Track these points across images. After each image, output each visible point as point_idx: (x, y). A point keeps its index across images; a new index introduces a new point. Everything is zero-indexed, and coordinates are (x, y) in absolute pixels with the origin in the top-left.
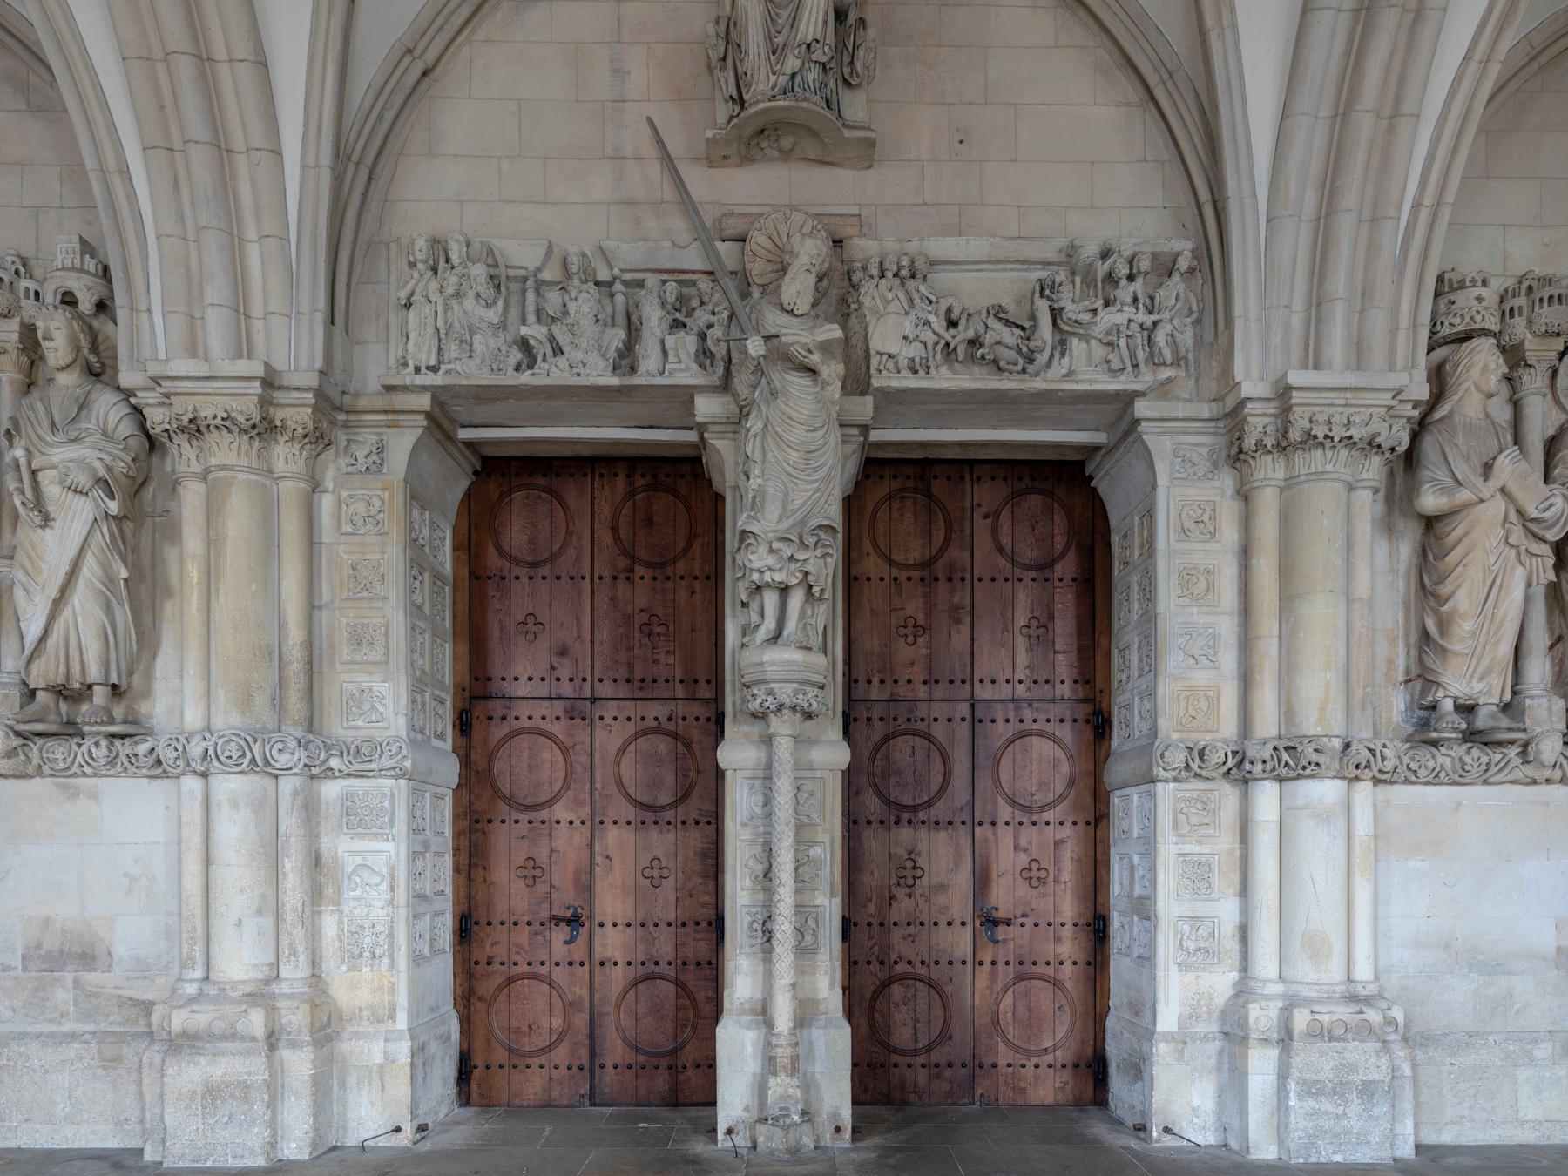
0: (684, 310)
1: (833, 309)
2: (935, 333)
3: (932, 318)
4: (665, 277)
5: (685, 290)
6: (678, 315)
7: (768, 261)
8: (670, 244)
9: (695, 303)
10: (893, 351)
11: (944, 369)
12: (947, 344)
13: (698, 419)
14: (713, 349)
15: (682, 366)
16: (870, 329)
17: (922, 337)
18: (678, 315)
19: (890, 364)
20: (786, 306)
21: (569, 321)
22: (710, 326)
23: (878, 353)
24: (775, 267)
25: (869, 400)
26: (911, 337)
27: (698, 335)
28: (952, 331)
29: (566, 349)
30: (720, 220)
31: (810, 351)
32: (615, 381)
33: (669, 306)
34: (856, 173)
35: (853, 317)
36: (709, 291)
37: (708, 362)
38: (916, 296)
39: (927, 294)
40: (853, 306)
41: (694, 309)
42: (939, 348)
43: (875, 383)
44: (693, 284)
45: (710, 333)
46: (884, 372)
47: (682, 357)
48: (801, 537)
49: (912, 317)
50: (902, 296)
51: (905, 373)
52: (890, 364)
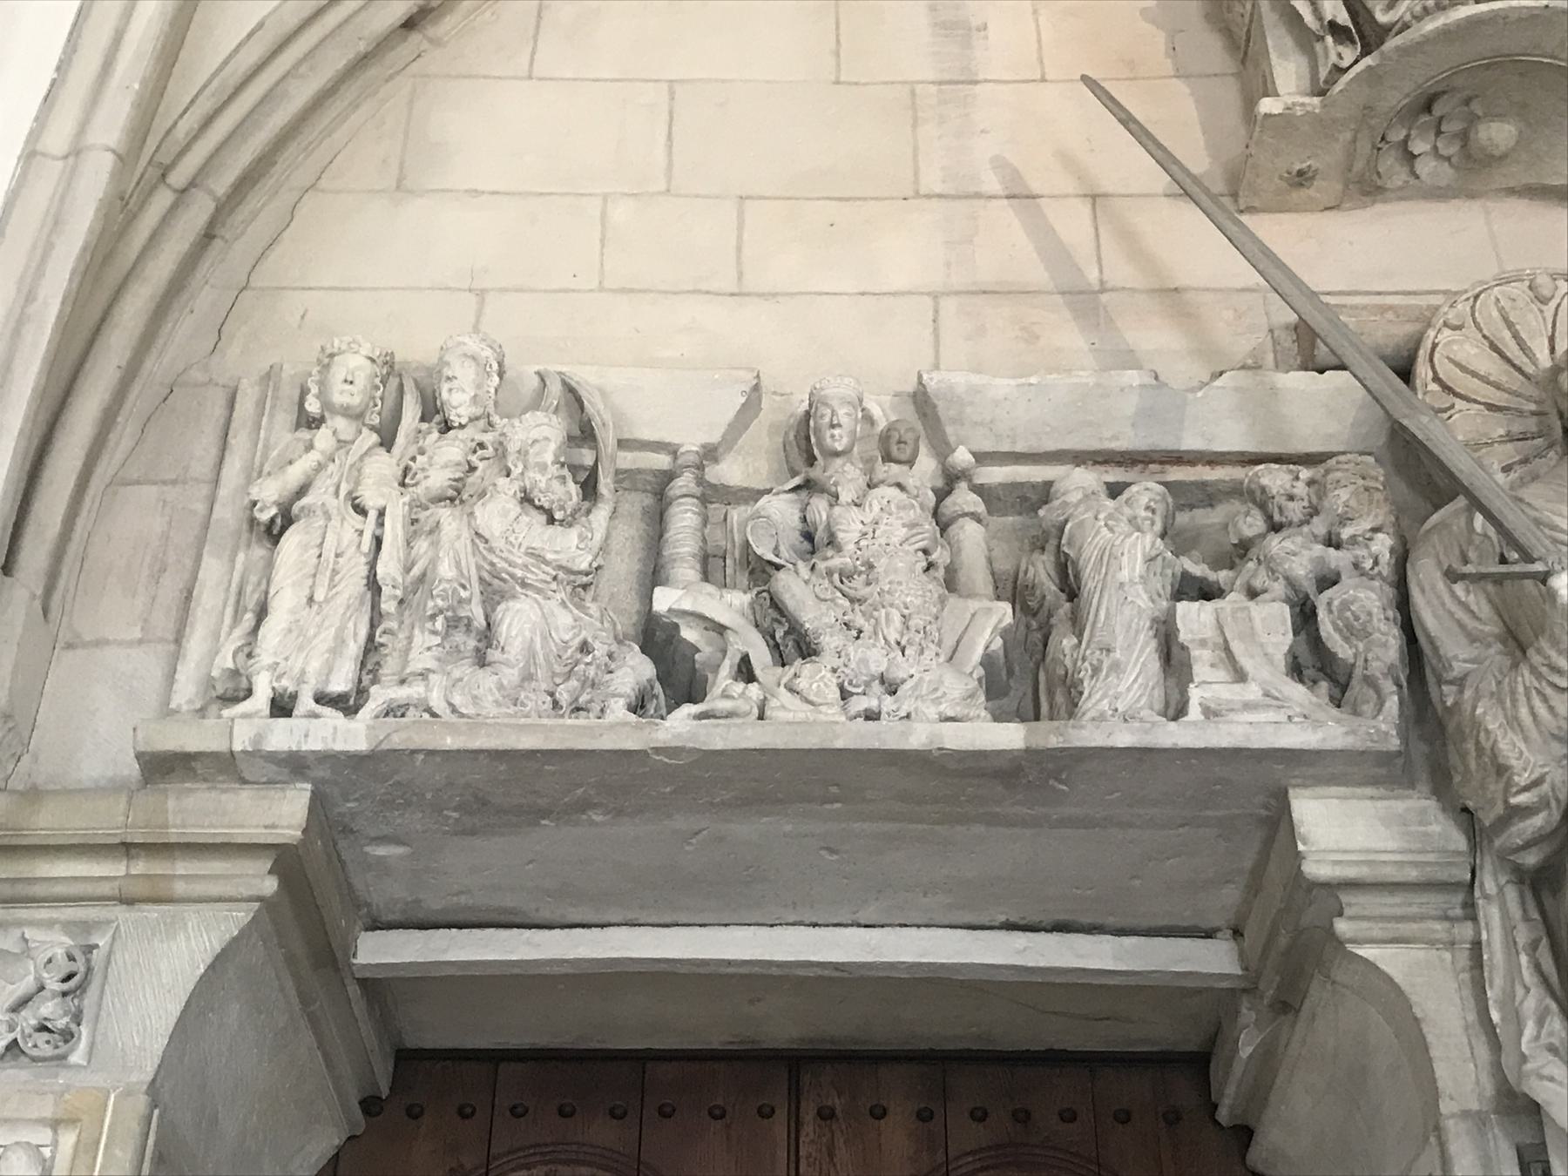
7: (1491, 407)
13: (1316, 869)
15: (1252, 692)
21: (836, 562)
22: (1327, 581)
27: (1288, 600)
29: (830, 641)
32: (1010, 736)
45: (1321, 602)
47: (1246, 663)
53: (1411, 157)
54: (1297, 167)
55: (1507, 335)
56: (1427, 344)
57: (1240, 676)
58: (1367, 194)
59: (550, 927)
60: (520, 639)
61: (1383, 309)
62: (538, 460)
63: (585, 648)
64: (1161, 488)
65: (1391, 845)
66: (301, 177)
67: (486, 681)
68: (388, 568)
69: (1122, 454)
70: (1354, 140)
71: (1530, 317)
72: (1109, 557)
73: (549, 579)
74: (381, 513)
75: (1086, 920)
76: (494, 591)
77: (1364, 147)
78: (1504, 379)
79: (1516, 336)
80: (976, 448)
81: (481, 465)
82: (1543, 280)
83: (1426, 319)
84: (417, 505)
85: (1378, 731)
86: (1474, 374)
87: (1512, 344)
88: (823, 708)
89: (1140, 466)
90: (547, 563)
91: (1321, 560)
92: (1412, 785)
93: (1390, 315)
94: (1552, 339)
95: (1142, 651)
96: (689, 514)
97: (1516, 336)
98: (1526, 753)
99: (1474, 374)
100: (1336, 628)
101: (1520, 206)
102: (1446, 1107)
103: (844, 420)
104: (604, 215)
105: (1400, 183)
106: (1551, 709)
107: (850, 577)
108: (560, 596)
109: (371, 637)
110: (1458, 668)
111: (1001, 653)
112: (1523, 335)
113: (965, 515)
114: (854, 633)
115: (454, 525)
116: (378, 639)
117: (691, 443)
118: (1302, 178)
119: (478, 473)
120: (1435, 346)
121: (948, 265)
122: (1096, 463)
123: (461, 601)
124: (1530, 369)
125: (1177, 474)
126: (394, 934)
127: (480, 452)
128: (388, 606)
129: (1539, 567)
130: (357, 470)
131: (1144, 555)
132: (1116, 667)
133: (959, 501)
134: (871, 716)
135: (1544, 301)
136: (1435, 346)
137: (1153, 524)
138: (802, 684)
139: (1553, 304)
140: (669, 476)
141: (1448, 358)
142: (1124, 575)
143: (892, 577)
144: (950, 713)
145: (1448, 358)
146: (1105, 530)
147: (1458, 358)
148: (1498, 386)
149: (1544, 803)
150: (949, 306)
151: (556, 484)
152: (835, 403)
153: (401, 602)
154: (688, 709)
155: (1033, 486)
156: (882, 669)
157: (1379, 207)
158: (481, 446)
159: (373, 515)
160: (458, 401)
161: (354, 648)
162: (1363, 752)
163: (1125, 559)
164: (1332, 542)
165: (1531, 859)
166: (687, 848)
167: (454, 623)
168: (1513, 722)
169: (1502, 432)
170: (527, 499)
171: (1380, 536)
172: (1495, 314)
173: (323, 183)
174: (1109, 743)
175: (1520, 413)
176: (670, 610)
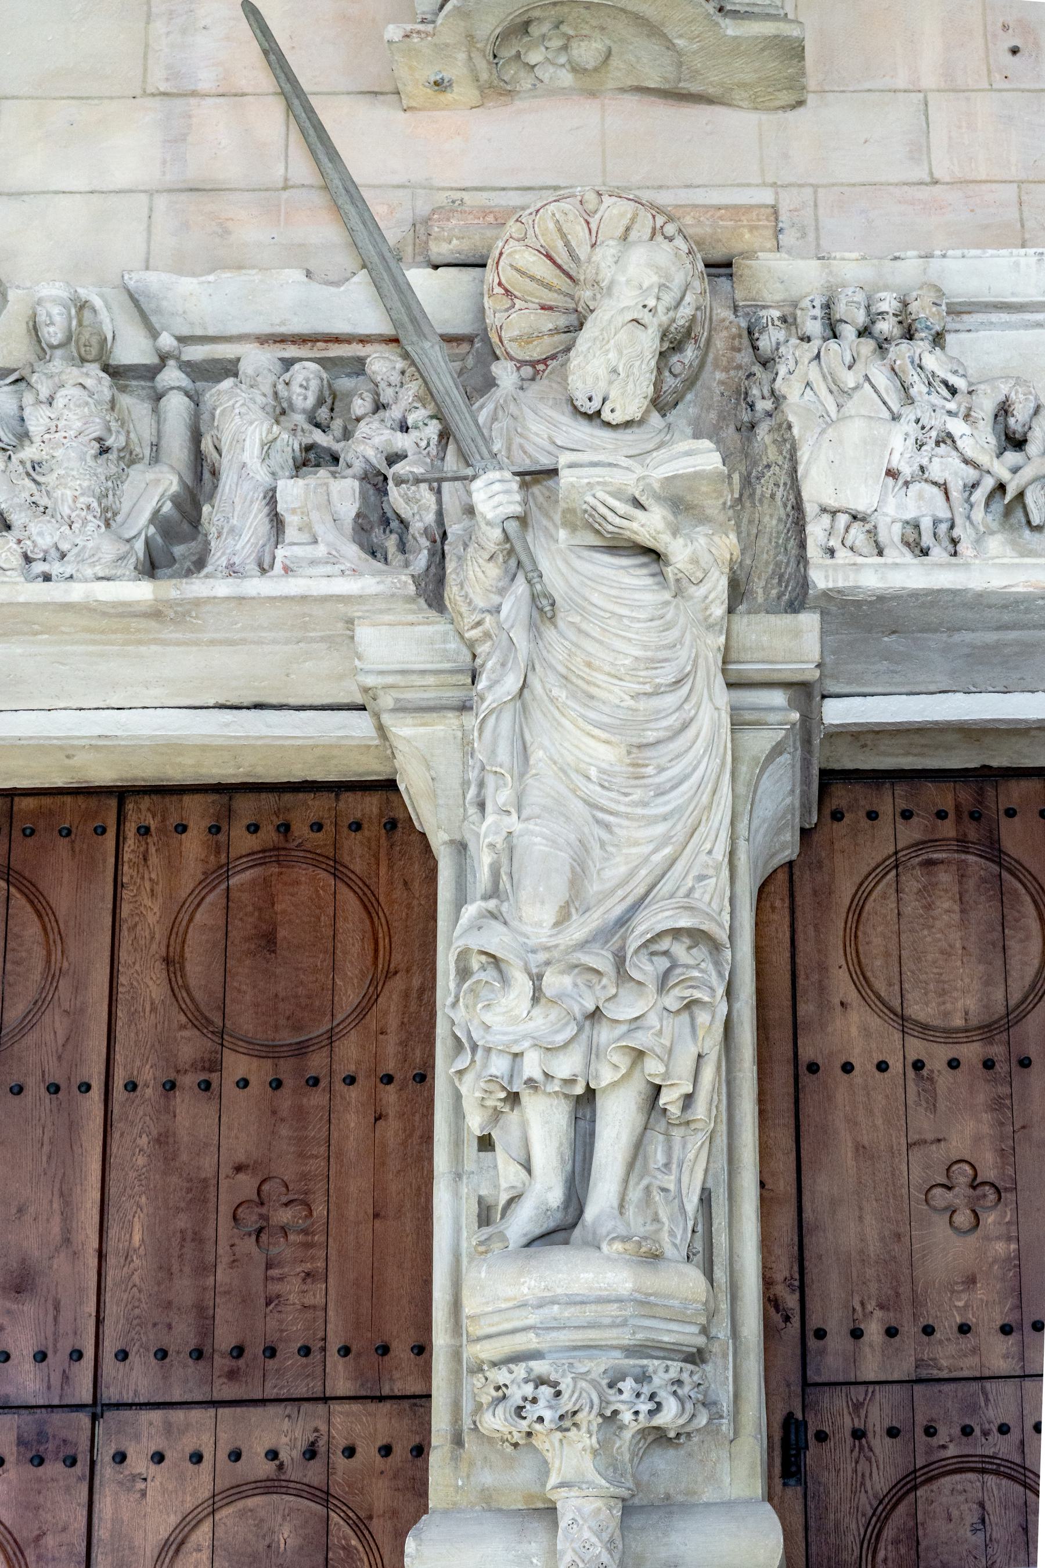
0: (337, 425)
1: (713, 415)
2: (966, 461)
3: (957, 427)
4: (291, 351)
5: (345, 383)
6: (319, 437)
8: (299, 275)
9: (360, 406)
10: (861, 506)
11: (995, 544)
12: (1001, 487)
14: (405, 511)
16: (804, 455)
17: (936, 471)
18: (319, 437)
19: (857, 534)
20: (581, 402)
23: (824, 510)
24: (562, 321)
25: (809, 621)
26: (907, 471)
28: (1012, 457)
30: (427, 221)
31: (638, 504)
33: (299, 419)
35: (762, 432)
36: (395, 378)
37: (391, 543)
38: (913, 377)
39: (942, 374)
40: (764, 405)
41: (358, 420)
42: (979, 496)
44: (358, 367)
46: (842, 554)
48: (620, 960)
49: (907, 426)
51: (897, 554)
52: (857, 534)
55: (560, 244)
71: (578, 228)
78: (555, 281)
79: (567, 244)
80: (177, 334)
97: (567, 244)
99: (532, 278)
112: (573, 244)
139: (598, 216)
141: (511, 266)
145: (511, 266)
147: (520, 264)
148: (549, 287)
164: (404, 428)
169: (551, 326)
172: (551, 225)
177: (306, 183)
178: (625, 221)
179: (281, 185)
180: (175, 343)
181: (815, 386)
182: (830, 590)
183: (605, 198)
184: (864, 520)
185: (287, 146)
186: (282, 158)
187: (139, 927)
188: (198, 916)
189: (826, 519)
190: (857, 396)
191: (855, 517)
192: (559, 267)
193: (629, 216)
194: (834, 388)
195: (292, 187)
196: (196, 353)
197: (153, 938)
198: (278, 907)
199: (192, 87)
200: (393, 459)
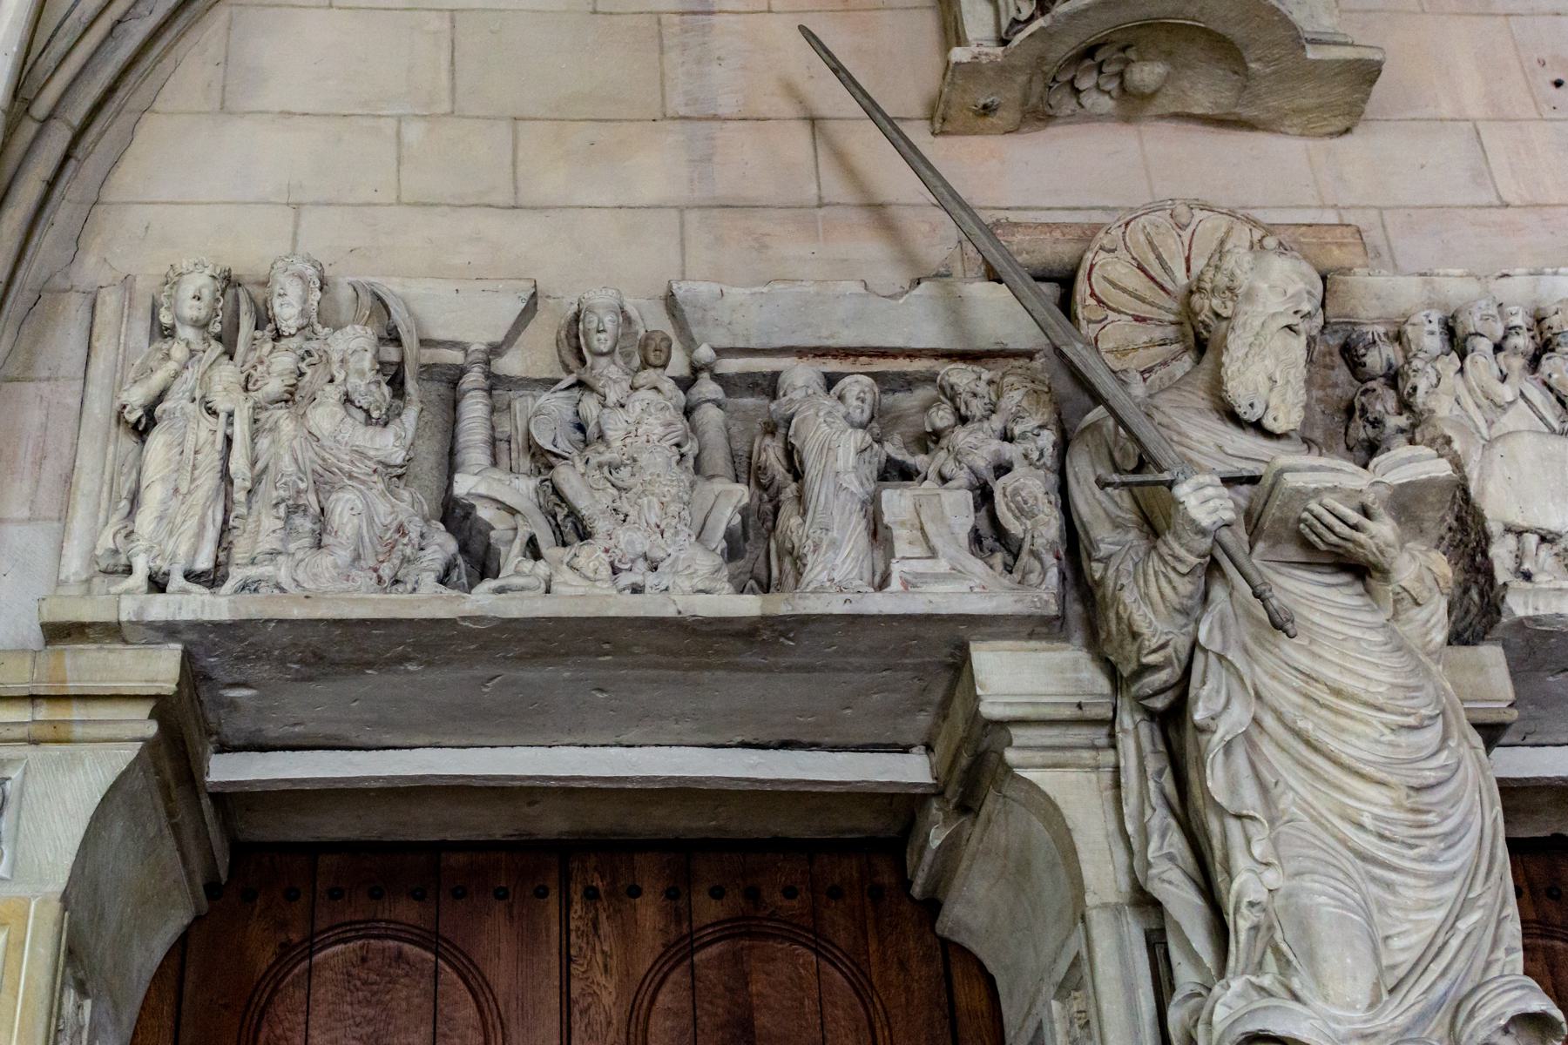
7: (1137, 319)
8: (857, 288)
13: (989, 710)
15: (942, 566)
21: (607, 457)
23: (1508, 530)
27: (972, 488)
32: (749, 606)
34: (1311, 143)
43: (1519, 605)
45: (998, 487)
47: (936, 542)
50: (1536, 394)
53: (1077, 92)
54: (982, 101)
55: (1152, 257)
56: (1086, 265)
57: (933, 554)
58: (1040, 120)
59: (367, 749)
60: (350, 525)
61: (1051, 227)
62: (358, 367)
63: (401, 530)
64: (867, 380)
65: (1052, 689)
66: (135, 103)
67: (325, 561)
68: (239, 463)
69: (837, 350)
70: (1030, 81)
72: (827, 449)
73: (370, 471)
74: (230, 415)
75: (805, 739)
76: (324, 481)
77: (1038, 88)
79: (1159, 257)
81: (309, 371)
82: (1182, 210)
83: (1088, 235)
84: (257, 408)
85: (1040, 599)
86: (1124, 290)
87: (1156, 263)
88: (598, 584)
89: (852, 359)
90: (370, 459)
91: (998, 453)
92: (1067, 639)
93: (1057, 234)
94: (1188, 260)
95: (855, 529)
96: (480, 406)
97: (1159, 257)
98: (1155, 622)
99: (1124, 290)
100: (1009, 509)
101: (1168, 129)
102: (1090, 900)
103: (609, 326)
104: (398, 134)
105: (1069, 112)
106: (1174, 588)
107: (617, 468)
108: (381, 486)
109: (225, 522)
110: (1104, 549)
111: (740, 527)
112: (1164, 256)
113: (709, 401)
114: (622, 517)
115: (291, 426)
116: (231, 523)
117: (479, 340)
118: (987, 110)
119: (307, 378)
120: (1092, 266)
121: (692, 181)
122: (816, 356)
123: (299, 492)
124: (1169, 286)
125: (881, 365)
126: (238, 755)
127: (308, 360)
128: (239, 496)
129: (1166, 476)
130: (204, 379)
131: (856, 448)
132: (833, 544)
133: (704, 390)
134: (637, 589)
135: (1183, 227)
136: (1092, 266)
137: (863, 411)
138: (581, 562)
139: (1190, 230)
140: (462, 371)
141: (1104, 278)
142: (840, 465)
143: (652, 470)
144: (701, 587)
145: (1104, 278)
146: (824, 427)
147: (1112, 276)
149: (1167, 663)
150: (693, 217)
151: (373, 387)
152: (601, 312)
153: (249, 491)
154: (489, 584)
155: (764, 375)
156: (646, 548)
157: (1052, 131)
158: (308, 353)
159: (223, 416)
160: (287, 313)
161: (212, 534)
162: (1029, 616)
163: (841, 450)
164: (1007, 437)
165: (1159, 703)
166: (486, 690)
167: (295, 509)
168: (1146, 597)
169: (1145, 338)
170: (347, 400)
171: (1045, 433)
172: (1142, 238)
173: (157, 106)
174: (827, 611)
175: (1160, 323)
176: (468, 494)
177: (841, 201)
178: (1220, 234)
179: (815, 202)
180: (712, 354)
181: (1462, 401)
182: (1528, 618)
183: (1196, 212)
184: (1552, 541)
185: (817, 166)
186: (814, 179)
187: (592, 1011)
188: (660, 997)
189: (1511, 540)
190: (1511, 412)
191: (1543, 539)
192: (1152, 279)
193: (1224, 229)
194: (1484, 402)
195: (827, 205)
196: (731, 366)
197: (609, 1023)
198: (753, 988)
199: (713, 112)
200: (1002, 469)
